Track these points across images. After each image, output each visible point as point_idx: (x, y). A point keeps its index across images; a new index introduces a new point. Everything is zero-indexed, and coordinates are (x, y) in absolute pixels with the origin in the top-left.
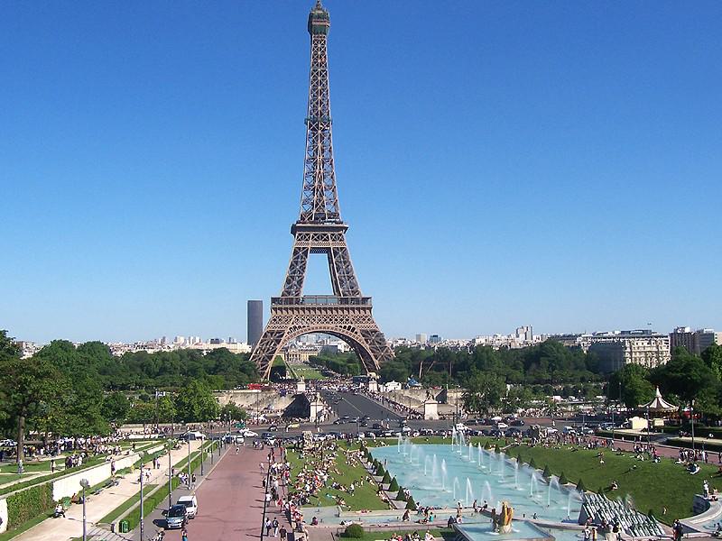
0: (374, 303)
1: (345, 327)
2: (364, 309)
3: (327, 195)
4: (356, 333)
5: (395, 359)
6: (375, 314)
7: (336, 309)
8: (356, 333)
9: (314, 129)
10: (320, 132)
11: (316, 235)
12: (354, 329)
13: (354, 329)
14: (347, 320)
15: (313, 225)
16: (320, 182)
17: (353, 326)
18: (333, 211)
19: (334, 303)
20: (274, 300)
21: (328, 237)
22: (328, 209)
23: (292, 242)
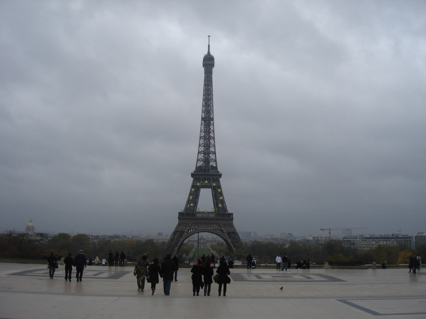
1: (218, 229)
2: (229, 219)
3: (212, 156)
4: (224, 233)
6: (235, 222)
7: (213, 219)
8: (224, 233)
10: (207, 122)
11: (204, 178)
12: (223, 231)
13: (223, 231)
14: (219, 226)
17: (222, 229)
18: (215, 165)
19: (213, 216)
20: (179, 213)
21: (210, 180)
22: (212, 164)
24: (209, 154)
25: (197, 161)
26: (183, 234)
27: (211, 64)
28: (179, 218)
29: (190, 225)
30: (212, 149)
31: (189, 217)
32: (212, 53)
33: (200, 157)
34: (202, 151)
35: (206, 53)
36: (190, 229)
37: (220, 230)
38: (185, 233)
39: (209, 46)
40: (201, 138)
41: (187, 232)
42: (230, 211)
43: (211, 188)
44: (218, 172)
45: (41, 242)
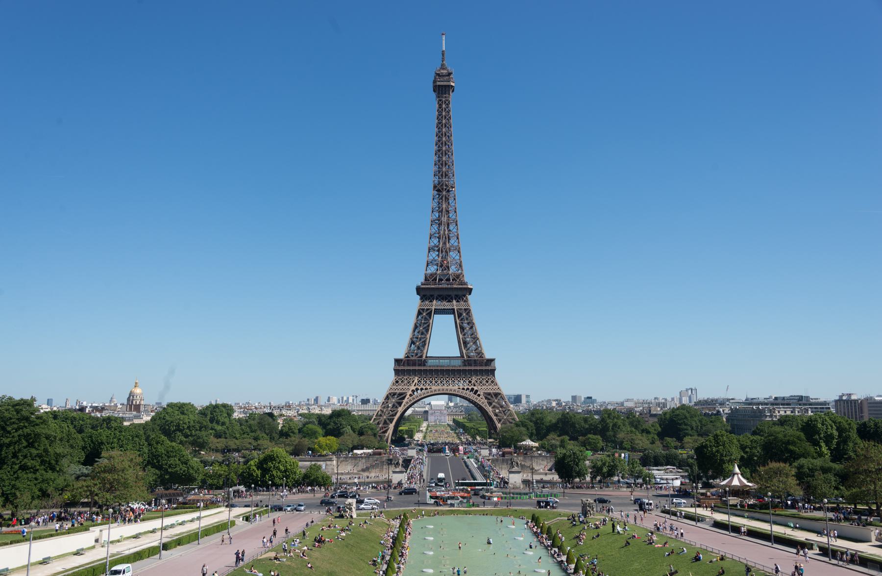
0: (497, 365)
1: (468, 389)
4: (479, 395)
5: (517, 425)
7: (459, 371)
8: (479, 395)
9: (438, 191)
10: (444, 193)
11: (439, 296)
12: (477, 391)
13: (477, 391)
14: (470, 382)
15: (437, 286)
16: (445, 243)
17: (475, 388)
19: (458, 364)
20: (398, 361)
23: (415, 302)
26: (404, 398)
29: (416, 381)
31: (412, 366)
33: (431, 258)
34: (435, 246)
36: (417, 389)
37: (472, 389)
38: (408, 396)
39: (443, 53)
41: (411, 395)
42: (488, 356)
43: (454, 313)
44: (466, 284)
45: (136, 421)
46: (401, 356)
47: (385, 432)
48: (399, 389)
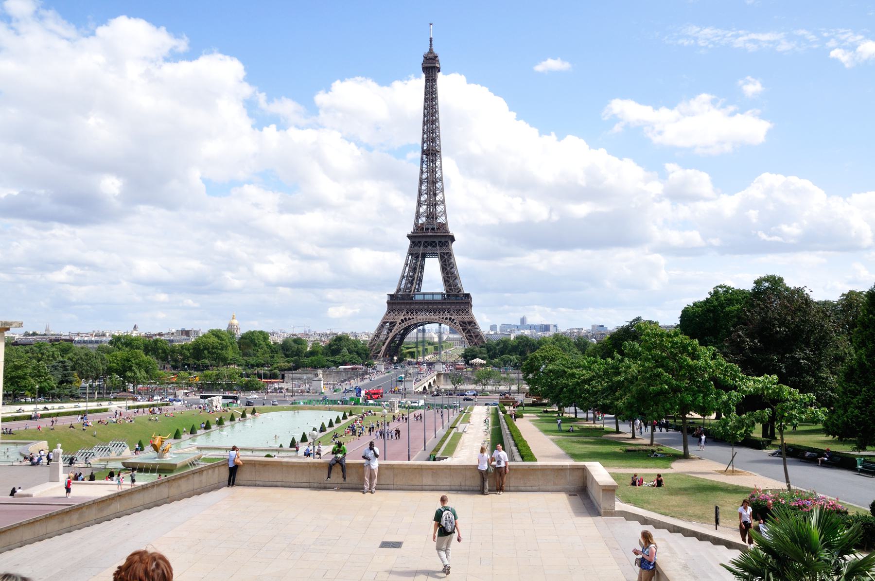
3: (439, 208)
19: (439, 297)
20: (391, 295)
22: (441, 220)
24: (435, 205)
25: (418, 216)
27: (434, 67)
28: (388, 303)
30: (439, 197)
31: (405, 301)
32: (436, 51)
35: (427, 51)
39: (431, 40)
40: (421, 182)
46: (393, 292)
47: (379, 353)
48: (392, 317)
